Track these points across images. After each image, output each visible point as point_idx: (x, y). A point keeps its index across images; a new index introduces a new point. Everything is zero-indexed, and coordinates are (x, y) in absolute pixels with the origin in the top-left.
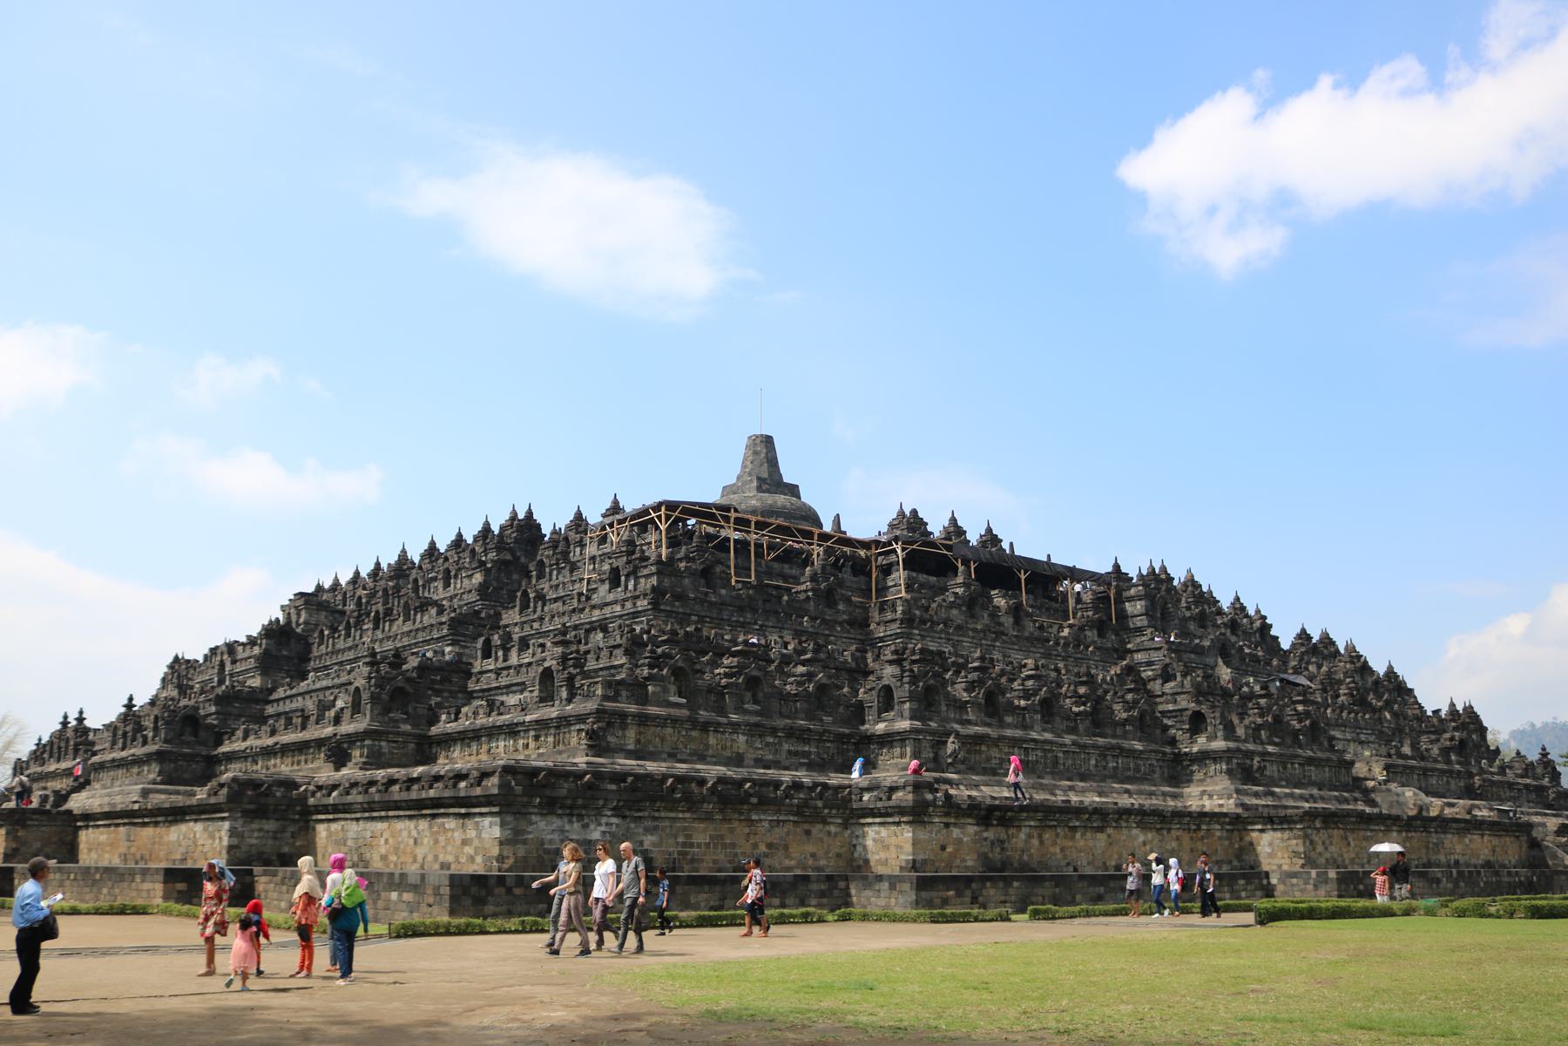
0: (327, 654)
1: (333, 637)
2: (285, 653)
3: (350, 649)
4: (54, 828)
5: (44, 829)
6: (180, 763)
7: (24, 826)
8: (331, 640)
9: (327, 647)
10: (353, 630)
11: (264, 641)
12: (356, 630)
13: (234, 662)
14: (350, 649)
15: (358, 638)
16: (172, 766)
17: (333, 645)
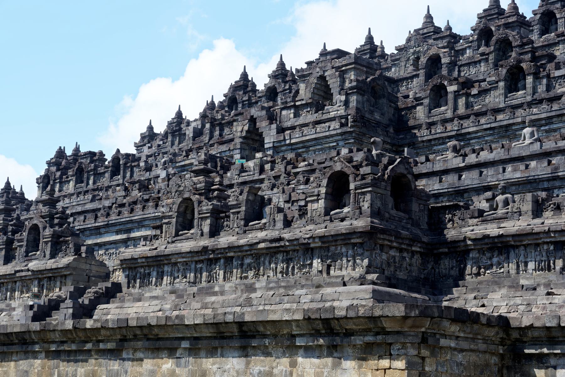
0: (461, 118)
1: (468, 95)
2: (377, 116)
3: (530, 104)
4: (473, 357)
5: (460, 357)
6: (392, 253)
7: (435, 349)
8: (462, 102)
9: (455, 108)
10: (530, 80)
11: (354, 99)
12: (537, 76)
13: (281, 130)
14: (530, 104)
15: (542, 88)
16: (384, 257)
17: (468, 105)
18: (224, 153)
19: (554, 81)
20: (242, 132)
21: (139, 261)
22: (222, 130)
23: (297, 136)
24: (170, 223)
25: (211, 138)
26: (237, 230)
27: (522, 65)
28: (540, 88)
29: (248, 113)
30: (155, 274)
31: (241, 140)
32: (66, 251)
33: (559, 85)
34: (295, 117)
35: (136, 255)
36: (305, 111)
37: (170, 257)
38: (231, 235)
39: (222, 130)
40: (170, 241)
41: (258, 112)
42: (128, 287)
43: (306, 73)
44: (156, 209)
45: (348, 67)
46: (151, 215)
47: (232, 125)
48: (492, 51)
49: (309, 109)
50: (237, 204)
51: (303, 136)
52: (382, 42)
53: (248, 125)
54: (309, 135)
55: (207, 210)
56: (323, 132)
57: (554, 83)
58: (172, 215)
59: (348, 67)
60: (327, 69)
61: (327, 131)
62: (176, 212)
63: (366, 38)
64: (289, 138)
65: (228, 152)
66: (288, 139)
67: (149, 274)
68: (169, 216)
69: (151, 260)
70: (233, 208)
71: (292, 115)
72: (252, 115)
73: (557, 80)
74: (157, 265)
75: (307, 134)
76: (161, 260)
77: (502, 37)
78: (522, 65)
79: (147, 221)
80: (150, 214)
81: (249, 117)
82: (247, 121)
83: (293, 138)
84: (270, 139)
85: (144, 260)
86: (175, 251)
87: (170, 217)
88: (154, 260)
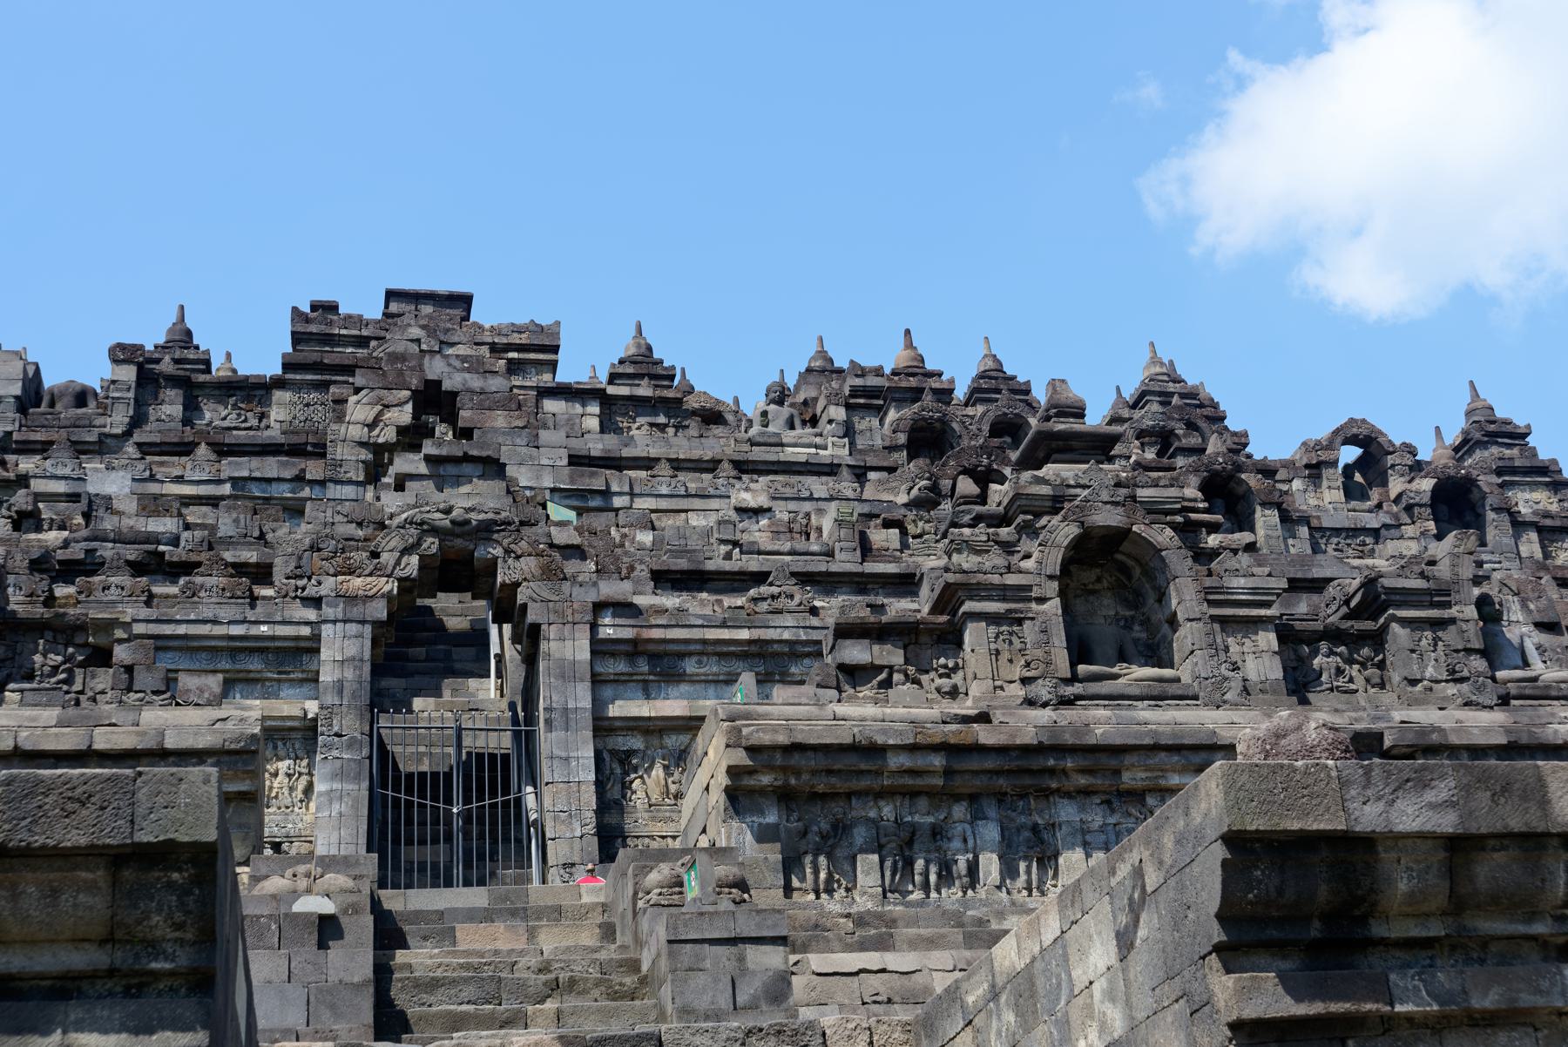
18: (264, 485)
19: (1322, 538)
20: (371, 426)
21: (895, 761)
22: (191, 408)
23: (664, 490)
24: (1020, 622)
25: (137, 421)
26: (1451, 689)
27: (1243, 476)
28: (1293, 546)
29: (412, 369)
30: (990, 832)
31: (365, 455)
32: (69, 681)
33: (1335, 550)
34: (602, 431)
35: (884, 732)
36: (641, 420)
37: (1129, 759)
38: (1436, 706)
39: (191, 408)
40: (1043, 690)
41: (467, 376)
42: (788, 890)
43: (343, 332)
44: (253, 606)
45: (532, 356)
46: (219, 630)
47: (265, 401)
48: (903, 445)
49: (662, 419)
50: (1428, 592)
51: (688, 496)
52: (229, 356)
53: (409, 408)
54: (720, 497)
55: (1254, 590)
56: (786, 499)
57: (1320, 541)
58: (1029, 588)
59: (532, 356)
60: (456, 339)
61: (804, 499)
62: (1051, 577)
63: (170, 331)
64: (626, 489)
65: (286, 486)
66: (620, 494)
67: (937, 833)
68: (1005, 587)
69: (990, 763)
70: (1400, 605)
71: (593, 423)
72: (430, 377)
73: (1330, 537)
74: (1000, 797)
75: (712, 491)
76: (1052, 772)
77: (931, 417)
78: (1243, 476)
79: (170, 655)
80: (215, 622)
81: (415, 382)
82: (407, 393)
83: (641, 495)
84: (538, 478)
85: (937, 761)
86: (1174, 735)
87: (1020, 593)
88: (1014, 765)
